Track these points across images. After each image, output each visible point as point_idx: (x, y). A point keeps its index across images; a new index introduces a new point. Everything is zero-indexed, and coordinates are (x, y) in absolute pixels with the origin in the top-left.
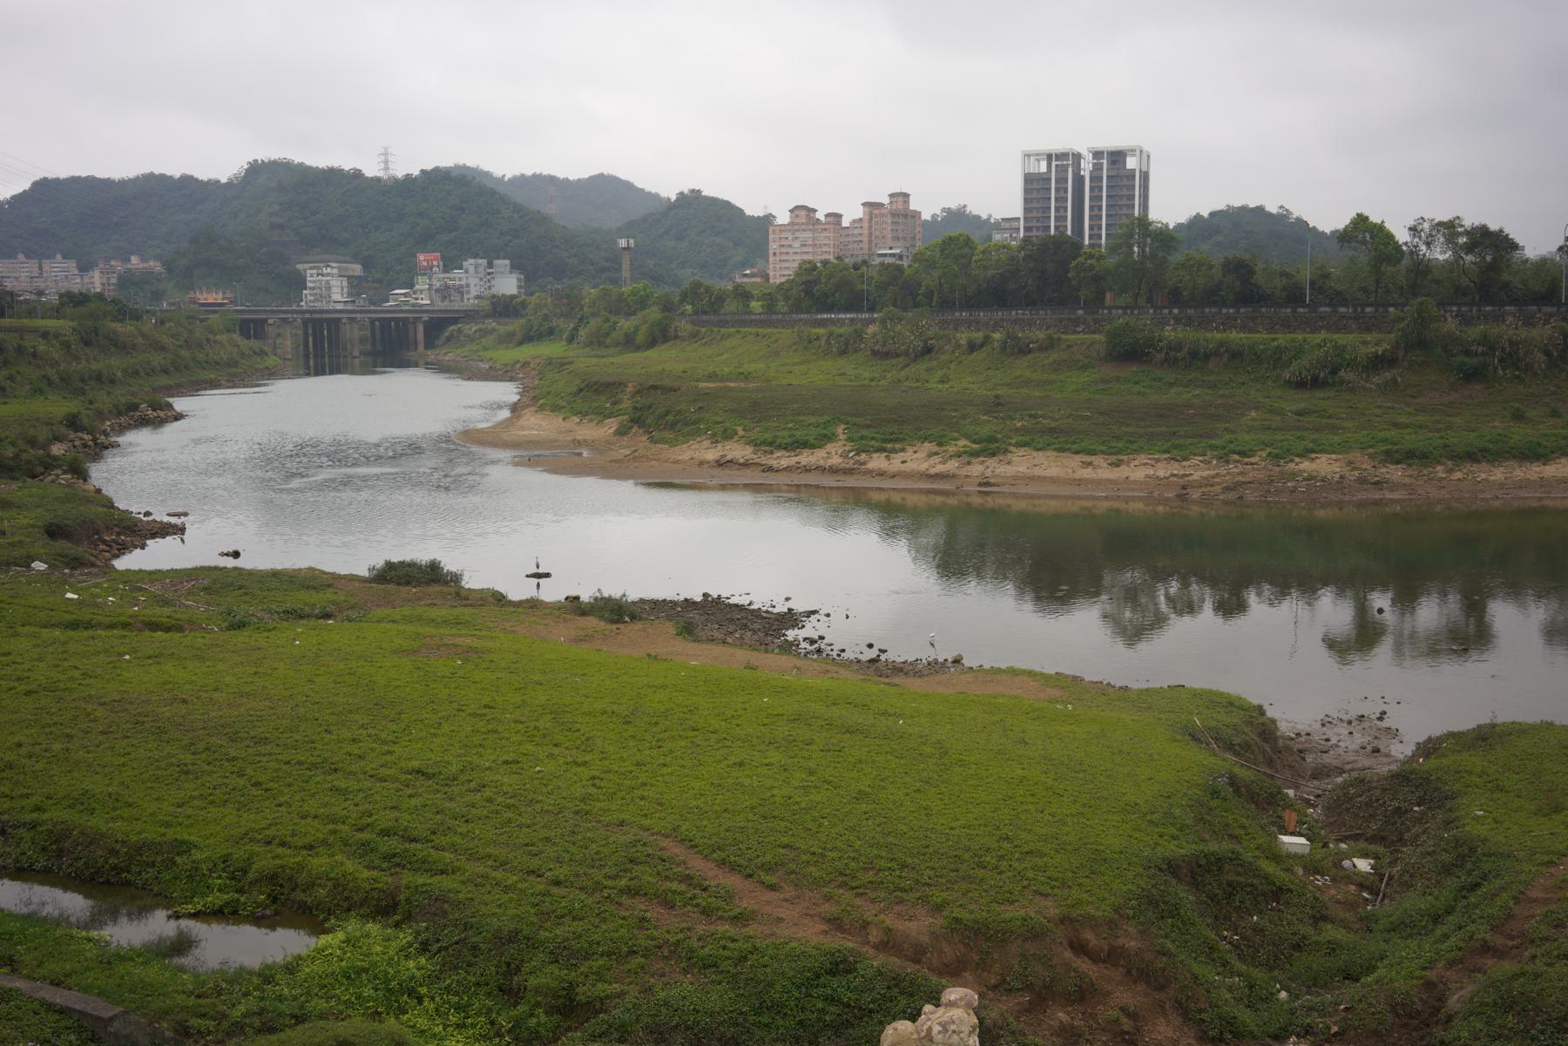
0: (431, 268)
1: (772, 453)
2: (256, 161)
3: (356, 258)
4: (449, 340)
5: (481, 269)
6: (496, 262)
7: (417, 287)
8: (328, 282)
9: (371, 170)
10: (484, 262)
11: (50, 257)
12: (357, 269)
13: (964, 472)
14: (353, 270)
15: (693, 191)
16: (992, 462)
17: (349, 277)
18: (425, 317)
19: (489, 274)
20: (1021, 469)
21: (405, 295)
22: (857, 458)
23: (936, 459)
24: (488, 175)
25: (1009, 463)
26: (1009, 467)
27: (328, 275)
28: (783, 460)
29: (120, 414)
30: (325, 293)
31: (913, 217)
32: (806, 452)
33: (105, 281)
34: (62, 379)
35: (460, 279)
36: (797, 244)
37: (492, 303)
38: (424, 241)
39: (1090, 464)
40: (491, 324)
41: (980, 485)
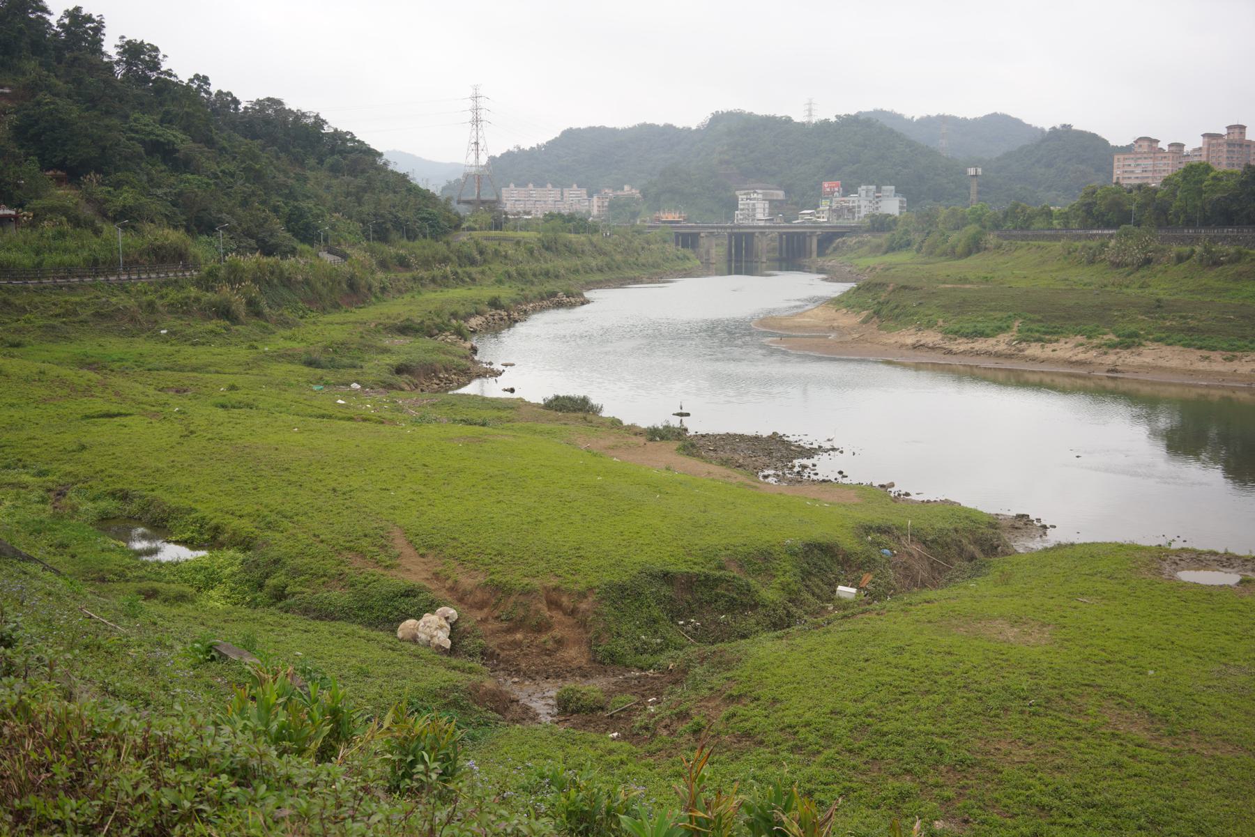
0: (833, 193)
1: (955, 340)
2: (717, 112)
3: (780, 187)
4: (835, 249)
5: (871, 194)
6: (884, 188)
7: (821, 208)
8: (754, 205)
9: (799, 117)
10: (873, 187)
11: (570, 186)
12: (780, 194)
13: (1099, 360)
14: (777, 195)
15: (1064, 126)
16: (1125, 353)
17: (771, 201)
18: (819, 231)
19: (878, 197)
20: (1147, 360)
21: (810, 214)
22: (1018, 346)
23: (1081, 349)
24: (899, 117)
25: (1139, 355)
26: (1137, 358)
27: (755, 199)
28: (962, 345)
29: (542, 299)
30: (751, 213)
31: (1248, 146)
32: (981, 340)
33: (600, 204)
34: (519, 274)
35: (854, 202)
36: (1138, 170)
37: (872, 221)
38: (831, 173)
39: (1207, 358)
40: (867, 237)
41: (1108, 371)
